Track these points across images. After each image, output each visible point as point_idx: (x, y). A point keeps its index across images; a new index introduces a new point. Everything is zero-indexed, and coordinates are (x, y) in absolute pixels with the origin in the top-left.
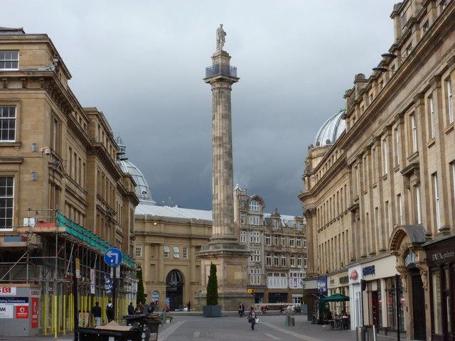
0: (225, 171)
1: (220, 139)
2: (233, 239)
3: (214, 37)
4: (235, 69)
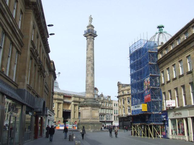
0: (91, 71)
1: (90, 58)
2: (94, 99)
3: (88, 20)
4: (96, 32)
